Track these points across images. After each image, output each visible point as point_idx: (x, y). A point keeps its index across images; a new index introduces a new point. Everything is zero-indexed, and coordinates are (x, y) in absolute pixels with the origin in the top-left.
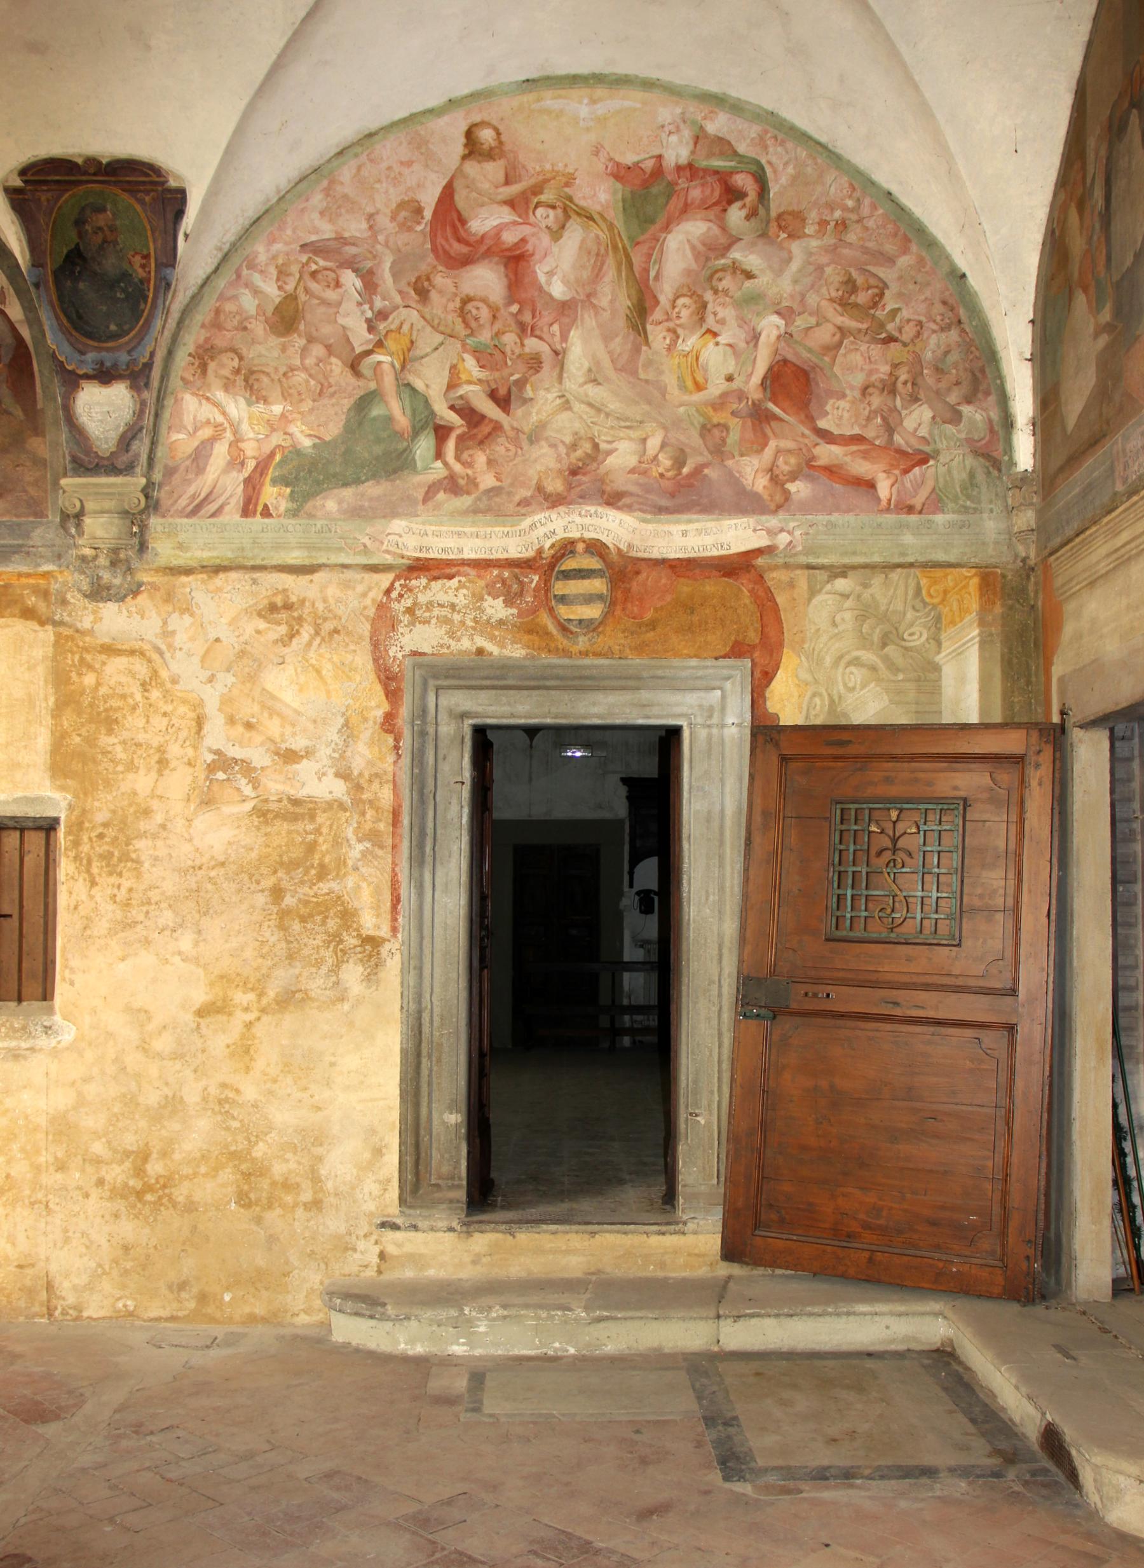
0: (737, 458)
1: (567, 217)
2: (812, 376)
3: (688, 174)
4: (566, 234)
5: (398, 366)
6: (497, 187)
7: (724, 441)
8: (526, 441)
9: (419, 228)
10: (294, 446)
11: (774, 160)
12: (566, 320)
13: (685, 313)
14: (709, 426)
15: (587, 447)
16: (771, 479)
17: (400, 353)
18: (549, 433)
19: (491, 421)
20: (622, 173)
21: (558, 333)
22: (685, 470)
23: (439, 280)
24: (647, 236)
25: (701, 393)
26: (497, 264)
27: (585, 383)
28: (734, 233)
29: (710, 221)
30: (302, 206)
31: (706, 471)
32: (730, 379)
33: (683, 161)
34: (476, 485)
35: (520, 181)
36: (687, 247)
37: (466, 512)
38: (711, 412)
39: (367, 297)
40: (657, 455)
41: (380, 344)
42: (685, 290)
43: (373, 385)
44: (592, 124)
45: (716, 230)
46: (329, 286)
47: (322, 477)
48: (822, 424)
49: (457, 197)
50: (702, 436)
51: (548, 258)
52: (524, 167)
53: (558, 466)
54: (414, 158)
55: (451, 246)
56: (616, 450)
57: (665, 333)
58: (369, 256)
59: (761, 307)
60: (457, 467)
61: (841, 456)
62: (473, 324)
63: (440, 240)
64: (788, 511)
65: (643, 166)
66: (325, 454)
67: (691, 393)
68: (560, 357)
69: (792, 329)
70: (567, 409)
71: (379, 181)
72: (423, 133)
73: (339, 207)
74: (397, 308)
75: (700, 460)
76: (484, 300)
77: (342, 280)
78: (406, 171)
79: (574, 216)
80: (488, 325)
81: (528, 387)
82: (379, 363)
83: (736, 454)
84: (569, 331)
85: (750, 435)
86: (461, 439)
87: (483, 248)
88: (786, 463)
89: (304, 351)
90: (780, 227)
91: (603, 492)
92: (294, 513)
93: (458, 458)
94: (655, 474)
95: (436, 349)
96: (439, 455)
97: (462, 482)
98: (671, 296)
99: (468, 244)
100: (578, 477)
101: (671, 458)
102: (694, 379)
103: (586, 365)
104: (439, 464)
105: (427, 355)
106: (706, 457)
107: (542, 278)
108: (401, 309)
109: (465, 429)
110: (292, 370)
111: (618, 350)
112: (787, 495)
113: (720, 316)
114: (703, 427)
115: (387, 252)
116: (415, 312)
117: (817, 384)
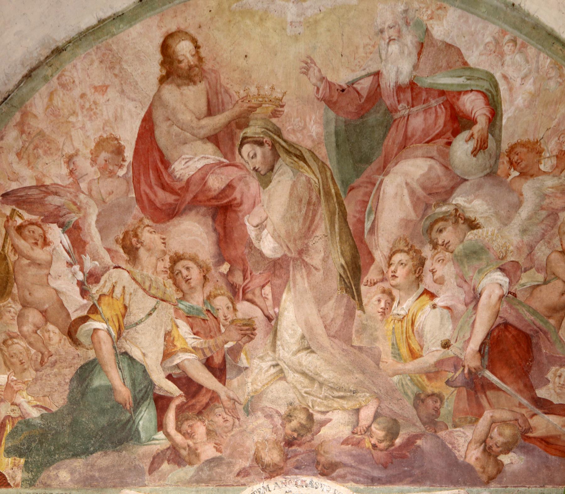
0: (450, 430)
1: (276, 157)
2: (534, 341)
3: (408, 95)
4: (276, 178)
5: (114, 334)
6: (199, 119)
7: (437, 411)
8: (243, 411)
9: (121, 173)
10: (22, 417)
11: (510, 72)
12: (277, 282)
13: (401, 272)
14: (422, 396)
15: (301, 417)
16: (484, 450)
17: (115, 319)
18: (265, 403)
19: (208, 391)
20: (336, 94)
21: (270, 297)
22: (398, 441)
23: (146, 235)
24: (363, 178)
25: (416, 361)
26: (204, 215)
27: (299, 351)
28: (458, 172)
29: (432, 158)
31: (419, 442)
32: (446, 345)
33: (404, 79)
34: (197, 456)
35: (223, 111)
36: (406, 192)
37: (189, 482)
38: (426, 382)
39: (76, 256)
40: (370, 426)
41: (94, 309)
42: (402, 246)
43: (92, 355)
44: (300, 30)
45: (439, 170)
46: (36, 244)
47: (53, 448)
48: (541, 393)
49: (157, 133)
50: (416, 407)
51: (256, 209)
52: (227, 91)
53: (275, 436)
54: (107, 83)
55: (156, 195)
56: (330, 420)
57: (380, 296)
58: (74, 207)
59: (484, 263)
60: (179, 438)
61: (560, 426)
62: (184, 286)
63: (144, 187)
64: (500, 483)
65: (358, 87)
66: (54, 425)
67: (405, 361)
68: (273, 323)
69: (516, 288)
70: (281, 379)
71: (74, 113)
72: (114, 47)
73: (36, 147)
74: (107, 269)
75: (413, 431)
76: (193, 259)
77: (50, 237)
78: (101, 99)
79: (283, 155)
80: (199, 288)
81: (243, 356)
82: (96, 330)
83: (450, 425)
84: (281, 294)
85: (464, 405)
86: (180, 409)
87: (189, 197)
88: (500, 434)
89: (20, 316)
90: (511, 163)
91: (318, 463)
92: (31, 483)
93: (178, 429)
94: (368, 445)
95: (150, 314)
96: (161, 426)
97: (184, 453)
98: (387, 252)
99: (173, 191)
100: (294, 448)
101: (384, 429)
102: (409, 345)
103: (299, 331)
104: (161, 435)
105: (141, 321)
106: (419, 428)
107: (252, 232)
108: (112, 270)
109: (183, 399)
110: (11, 338)
111: (332, 315)
112: (500, 466)
113: (438, 275)
114: (417, 396)
115: (92, 202)
116: (126, 274)
117: (540, 350)
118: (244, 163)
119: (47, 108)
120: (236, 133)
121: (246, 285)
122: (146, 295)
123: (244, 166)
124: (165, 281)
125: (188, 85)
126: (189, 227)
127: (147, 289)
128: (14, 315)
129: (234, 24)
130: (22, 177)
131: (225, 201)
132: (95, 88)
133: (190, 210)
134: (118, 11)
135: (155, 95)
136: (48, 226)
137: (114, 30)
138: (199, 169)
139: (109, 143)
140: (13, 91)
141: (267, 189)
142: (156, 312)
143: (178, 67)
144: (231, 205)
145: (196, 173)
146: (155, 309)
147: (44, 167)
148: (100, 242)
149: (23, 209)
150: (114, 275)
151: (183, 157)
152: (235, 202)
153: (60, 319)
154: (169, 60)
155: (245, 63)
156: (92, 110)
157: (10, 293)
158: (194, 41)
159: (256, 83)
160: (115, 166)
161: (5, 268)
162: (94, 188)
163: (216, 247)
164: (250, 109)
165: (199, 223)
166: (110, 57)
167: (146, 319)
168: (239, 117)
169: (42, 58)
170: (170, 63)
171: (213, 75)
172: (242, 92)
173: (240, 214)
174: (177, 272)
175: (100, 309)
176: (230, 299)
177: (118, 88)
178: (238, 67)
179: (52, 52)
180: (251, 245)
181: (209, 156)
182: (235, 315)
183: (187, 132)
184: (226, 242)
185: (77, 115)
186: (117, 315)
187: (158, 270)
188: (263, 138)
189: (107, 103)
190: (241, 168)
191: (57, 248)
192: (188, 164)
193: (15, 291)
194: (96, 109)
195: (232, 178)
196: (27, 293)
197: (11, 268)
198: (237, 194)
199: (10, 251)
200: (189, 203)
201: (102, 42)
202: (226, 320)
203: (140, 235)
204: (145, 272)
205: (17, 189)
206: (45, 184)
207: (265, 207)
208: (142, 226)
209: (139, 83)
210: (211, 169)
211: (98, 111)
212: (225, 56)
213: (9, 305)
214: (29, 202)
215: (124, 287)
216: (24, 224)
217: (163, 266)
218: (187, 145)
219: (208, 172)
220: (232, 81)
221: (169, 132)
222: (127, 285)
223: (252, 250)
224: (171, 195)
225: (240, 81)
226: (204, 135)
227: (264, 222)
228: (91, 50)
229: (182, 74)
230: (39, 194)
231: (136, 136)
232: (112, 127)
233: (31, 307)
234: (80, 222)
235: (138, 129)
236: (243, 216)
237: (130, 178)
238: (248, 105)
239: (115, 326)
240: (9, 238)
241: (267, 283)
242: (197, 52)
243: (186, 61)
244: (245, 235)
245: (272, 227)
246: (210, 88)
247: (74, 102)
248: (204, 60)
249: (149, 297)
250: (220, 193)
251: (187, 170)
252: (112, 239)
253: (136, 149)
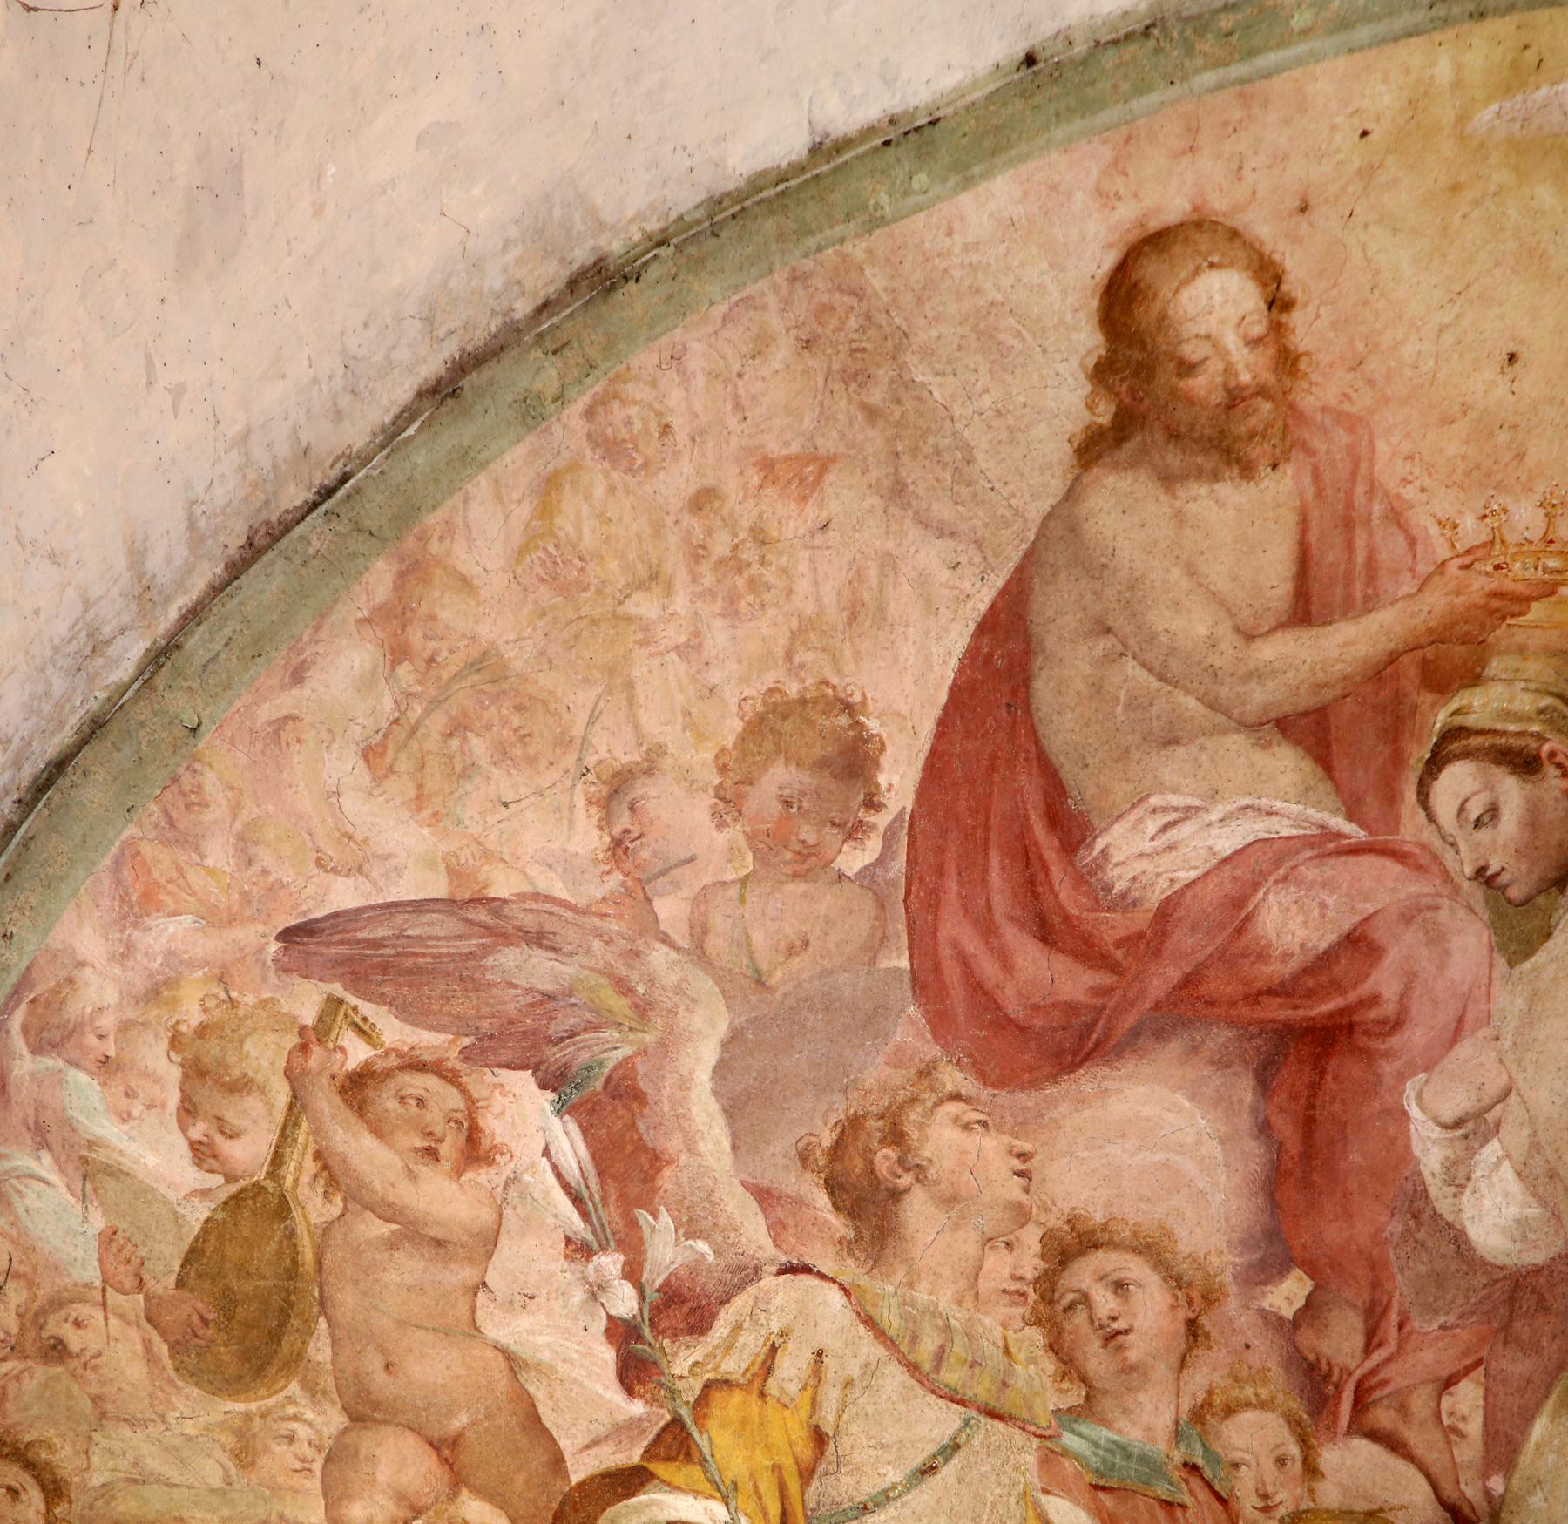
6: (1249, 636)
9: (855, 859)
17: (768, 1487)
21: (1474, 1427)
26: (1222, 1063)
30: (266, 713)
35: (1370, 604)
39: (610, 1215)
46: (431, 1154)
49: (1043, 689)
51: (1464, 1050)
52: (1396, 517)
54: (829, 443)
55: (1007, 966)
58: (619, 1004)
62: (1096, 1360)
63: (955, 929)
71: (654, 578)
72: (876, 280)
73: (459, 727)
74: (748, 1274)
76: (1152, 1249)
77: (494, 1127)
80: (1162, 1372)
87: (1161, 979)
95: (928, 1470)
99: (1087, 951)
105: (884, 1498)
108: (769, 1281)
115: (703, 984)
116: (835, 1297)
118: (1437, 843)
119: (523, 551)
120: (1415, 708)
121: (1373, 1372)
122: (919, 1391)
123: (1436, 858)
124: (1010, 1334)
125: (1216, 477)
126: (1147, 1111)
127: (927, 1366)
128: (309, 1452)
129: (1477, 203)
130: (386, 857)
131: (1328, 1006)
132: (768, 466)
133: (1161, 1035)
134: (913, 102)
135: (1049, 517)
136: (489, 1078)
137: (884, 199)
138: (1226, 860)
139: (810, 723)
140: (365, 460)
141: (1527, 965)
142: (955, 1461)
143: (1173, 392)
144: (1351, 1028)
145: (1206, 874)
146: (953, 1447)
147: (491, 820)
148: (727, 1159)
149: (381, 999)
150: (778, 1300)
151: (1154, 800)
152: (1373, 1014)
153: (520, 1479)
154: (1136, 355)
155: (1501, 391)
156: (741, 567)
157: (299, 1355)
158: (1268, 274)
159: (1541, 487)
160: (827, 829)
161: (279, 1254)
162: (718, 922)
163: (1260, 1201)
164: (1496, 603)
165: (1193, 1097)
166: (852, 323)
167: (908, 1490)
168: (1440, 635)
169: (523, 308)
170: (1136, 374)
171: (1342, 437)
172: (1469, 522)
173: (1388, 1068)
174: (1071, 1297)
175: (701, 1441)
176: (1295, 1424)
177: (875, 473)
178: (1465, 408)
179: (573, 284)
180: (1420, 1204)
181: (1278, 804)
182: (1311, 1491)
183: (1188, 692)
184: (1307, 1185)
185: (669, 590)
186: (777, 1469)
187: (984, 1285)
188: (1540, 737)
189: (819, 540)
190: (1419, 868)
191: (527, 1177)
192: (1173, 834)
193: (320, 1350)
194: (763, 562)
195: (1370, 908)
196: (374, 1363)
197: (308, 1255)
198: (1385, 981)
199: (305, 1179)
200: (1157, 1006)
201: (819, 249)
202: (1266, 1509)
203: (915, 1135)
204: (922, 1295)
205: (358, 911)
206: (492, 893)
207: (1507, 1044)
208: (930, 1098)
209: (979, 455)
210: (1277, 863)
211: (769, 575)
212: (1408, 351)
213: (291, 1410)
214: (410, 972)
215: (820, 1354)
216: (379, 1065)
217: (1006, 1272)
218: (1180, 751)
219: (1264, 875)
220: (1430, 469)
221: (1097, 688)
222: (832, 1344)
223: (1419, 1225)
224: (1078, 968)
225: (1468, 473)
226: (1266, 708)
227: (1490, 1108)
228: (763, 285)
229: (1192, 428)
230: (459, 937)
231: (943, 697)
232: (834, 658)
233: (386, 1422)
234: (642, 1067)
235: (954, 663)
236: (1402, 1077)
237: (892, 883)
238: (1493, 584)
239: (765, 1514)
240: (304, 1125)
241: (1467, 1371)
242: (1277, 328)
243: (1216, 366)
244: (1401, 1156)
245: (1526, 1131)
246: (1319, 494)
247: (658, 529)
248: (1303, 365)
249: (931, 1398)
250: (1306, 971)
251: (1166, 861)
252: (782, 1146)
253: (933, 753)
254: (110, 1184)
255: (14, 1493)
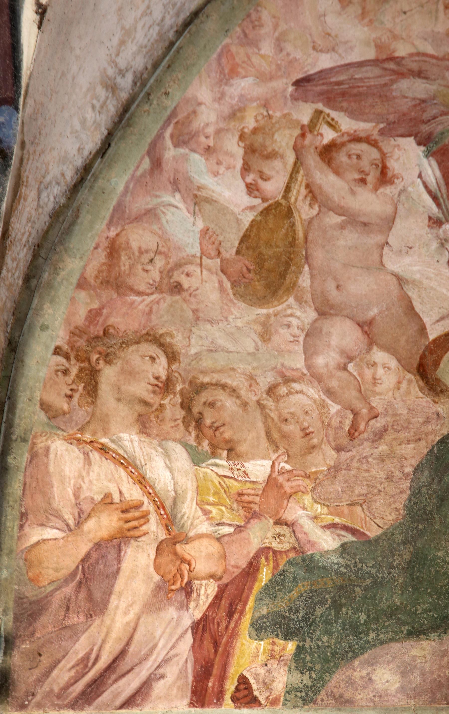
46: (363, 181)
128: (297, 332)
130: (346, 43)
136: (392, 142)
147: (397, 20)
149: (341, 109)
157: (294, 284)
161: (286, 235)
191: (410, 189)
196: (331, 286)
197: (300, 234)
199: (301, 198)
205: (331, 69)
206: (397, 54)
213: (289, 312)
214: (355, 95)
216: (339, 141)
230: (380, 77)
233: (336, 315)
240: (302, 172)
254: (207, 207)
255: (153, 359)
